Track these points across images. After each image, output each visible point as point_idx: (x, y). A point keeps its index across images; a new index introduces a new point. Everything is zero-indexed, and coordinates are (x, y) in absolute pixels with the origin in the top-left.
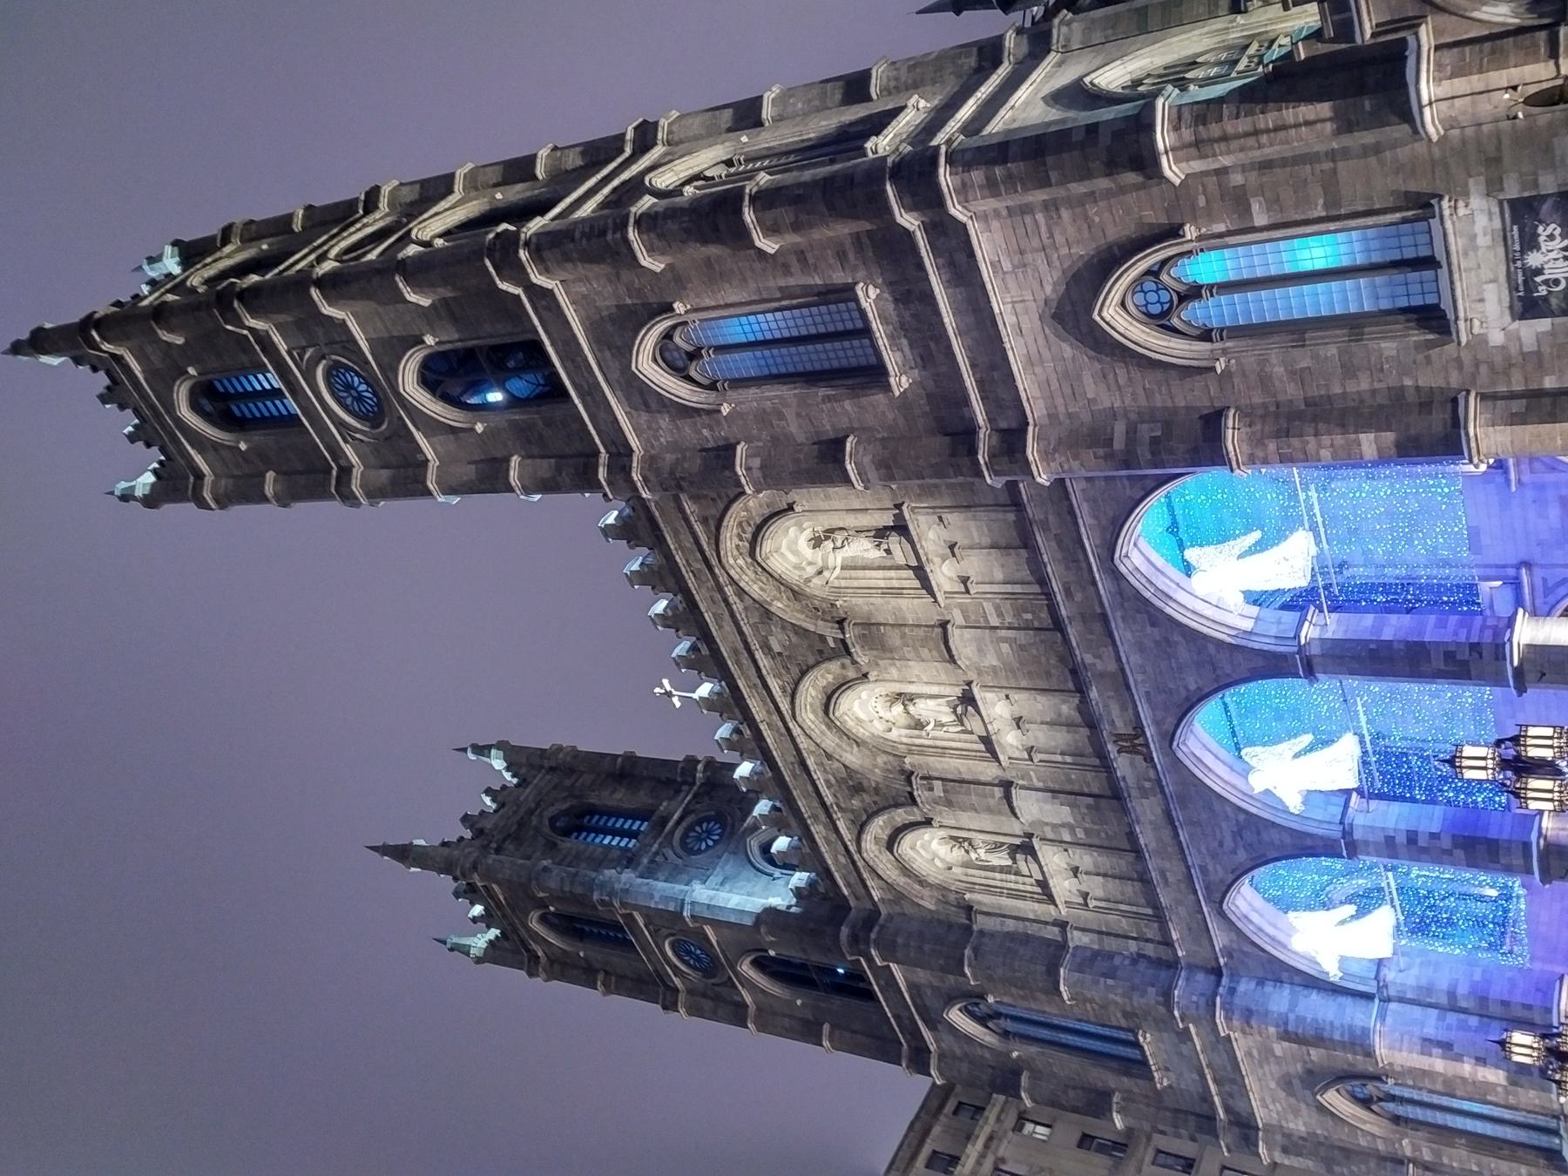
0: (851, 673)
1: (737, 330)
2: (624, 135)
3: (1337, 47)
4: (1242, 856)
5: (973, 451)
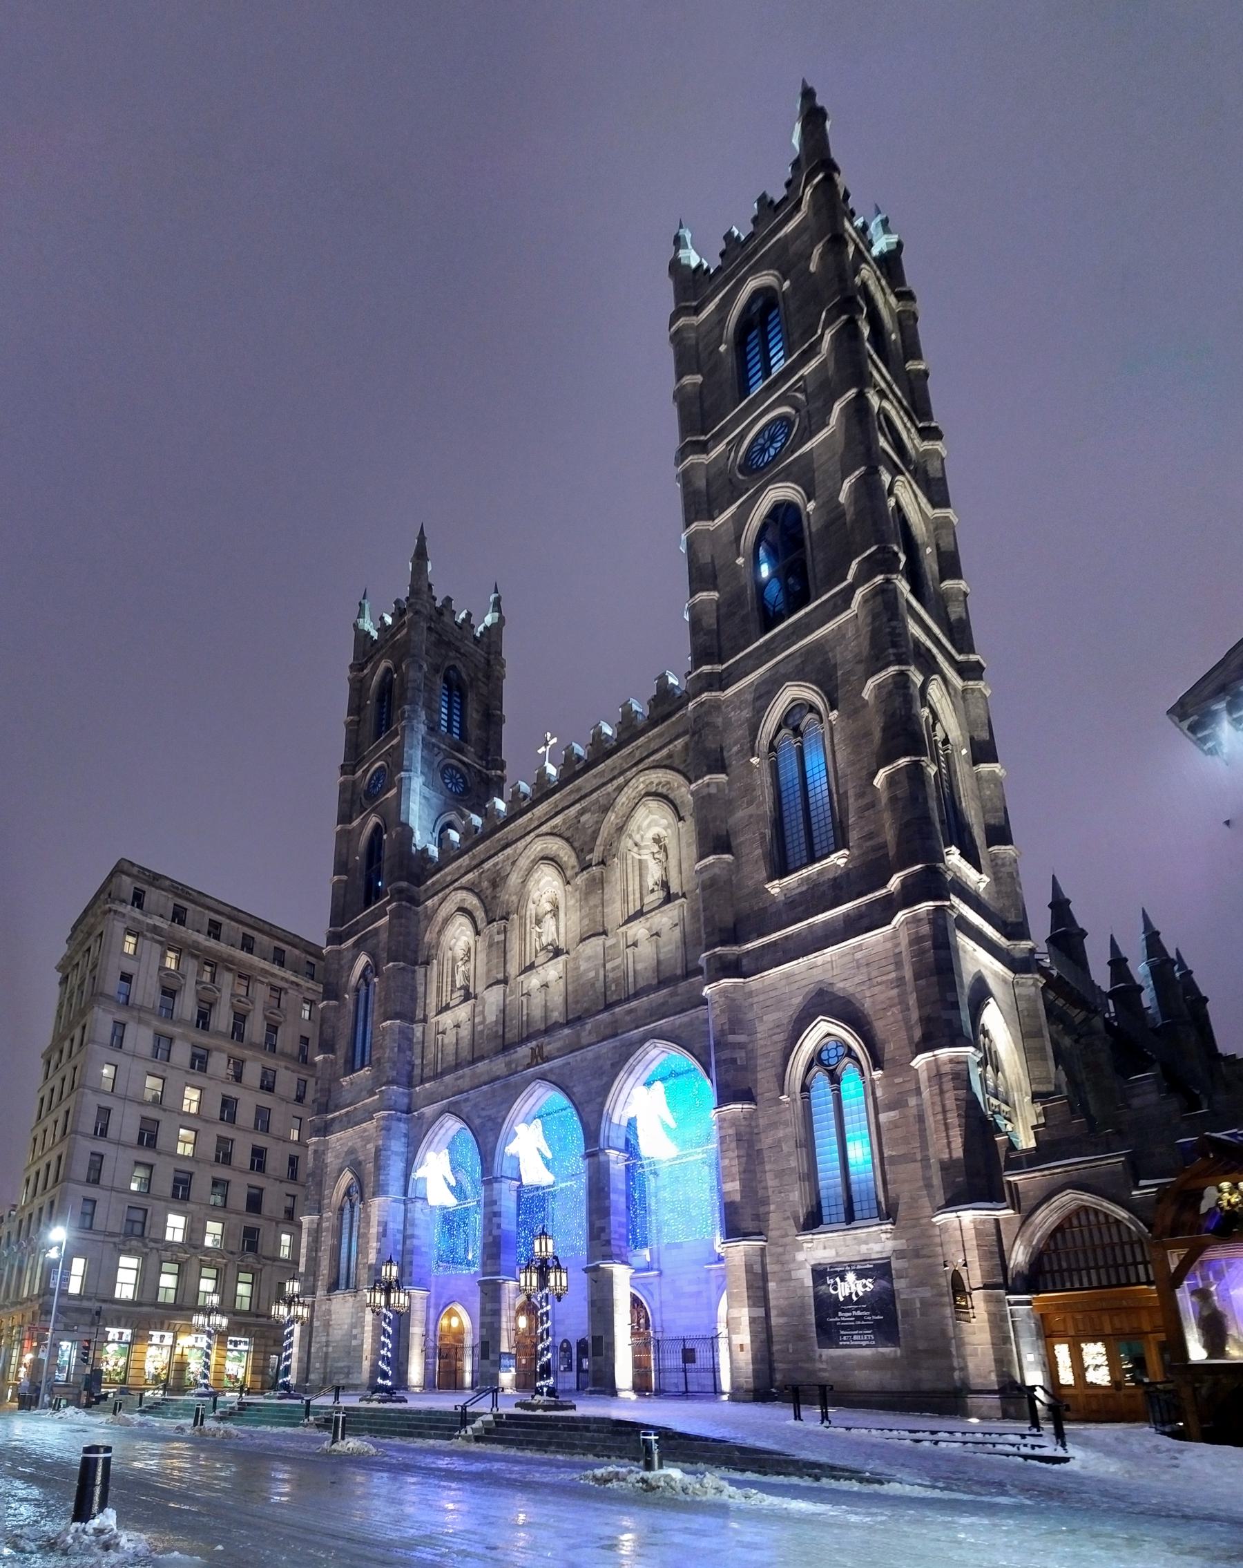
0: (569, 873)
1: (816, 764)
2: (974, 653)
3: (1002, 1160)
4: (477, 1121)
5: (723, 943)
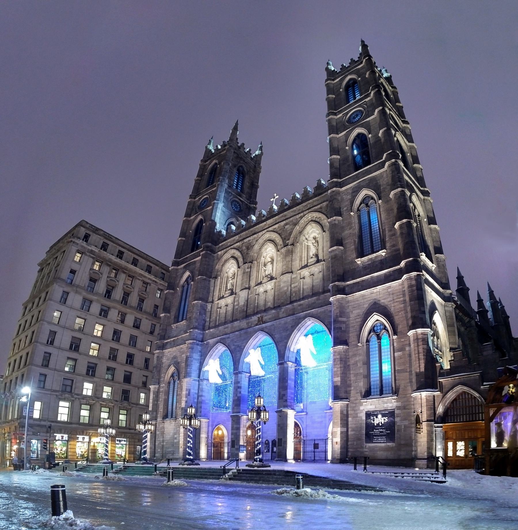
0: (279, 247)
1: (374, 217)
2: (426, 188)
3: (438, 373)
4: (233, 347)
5: (339, 281)
